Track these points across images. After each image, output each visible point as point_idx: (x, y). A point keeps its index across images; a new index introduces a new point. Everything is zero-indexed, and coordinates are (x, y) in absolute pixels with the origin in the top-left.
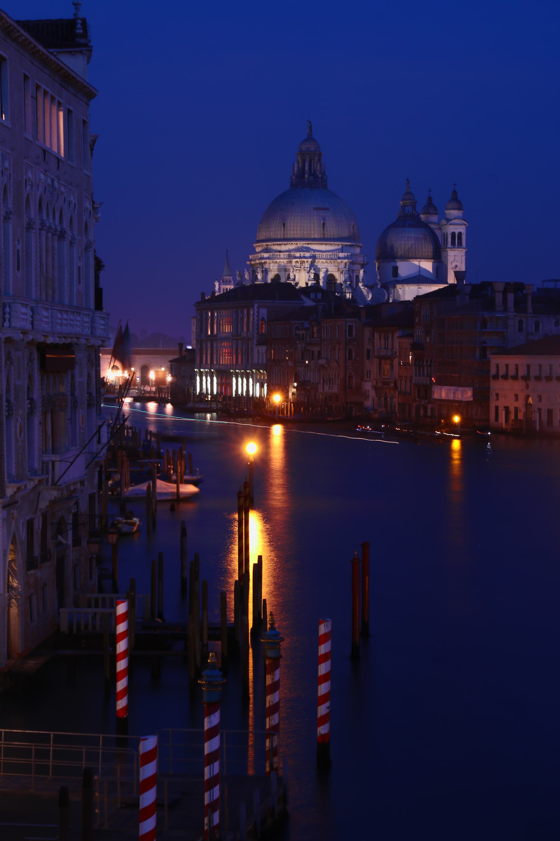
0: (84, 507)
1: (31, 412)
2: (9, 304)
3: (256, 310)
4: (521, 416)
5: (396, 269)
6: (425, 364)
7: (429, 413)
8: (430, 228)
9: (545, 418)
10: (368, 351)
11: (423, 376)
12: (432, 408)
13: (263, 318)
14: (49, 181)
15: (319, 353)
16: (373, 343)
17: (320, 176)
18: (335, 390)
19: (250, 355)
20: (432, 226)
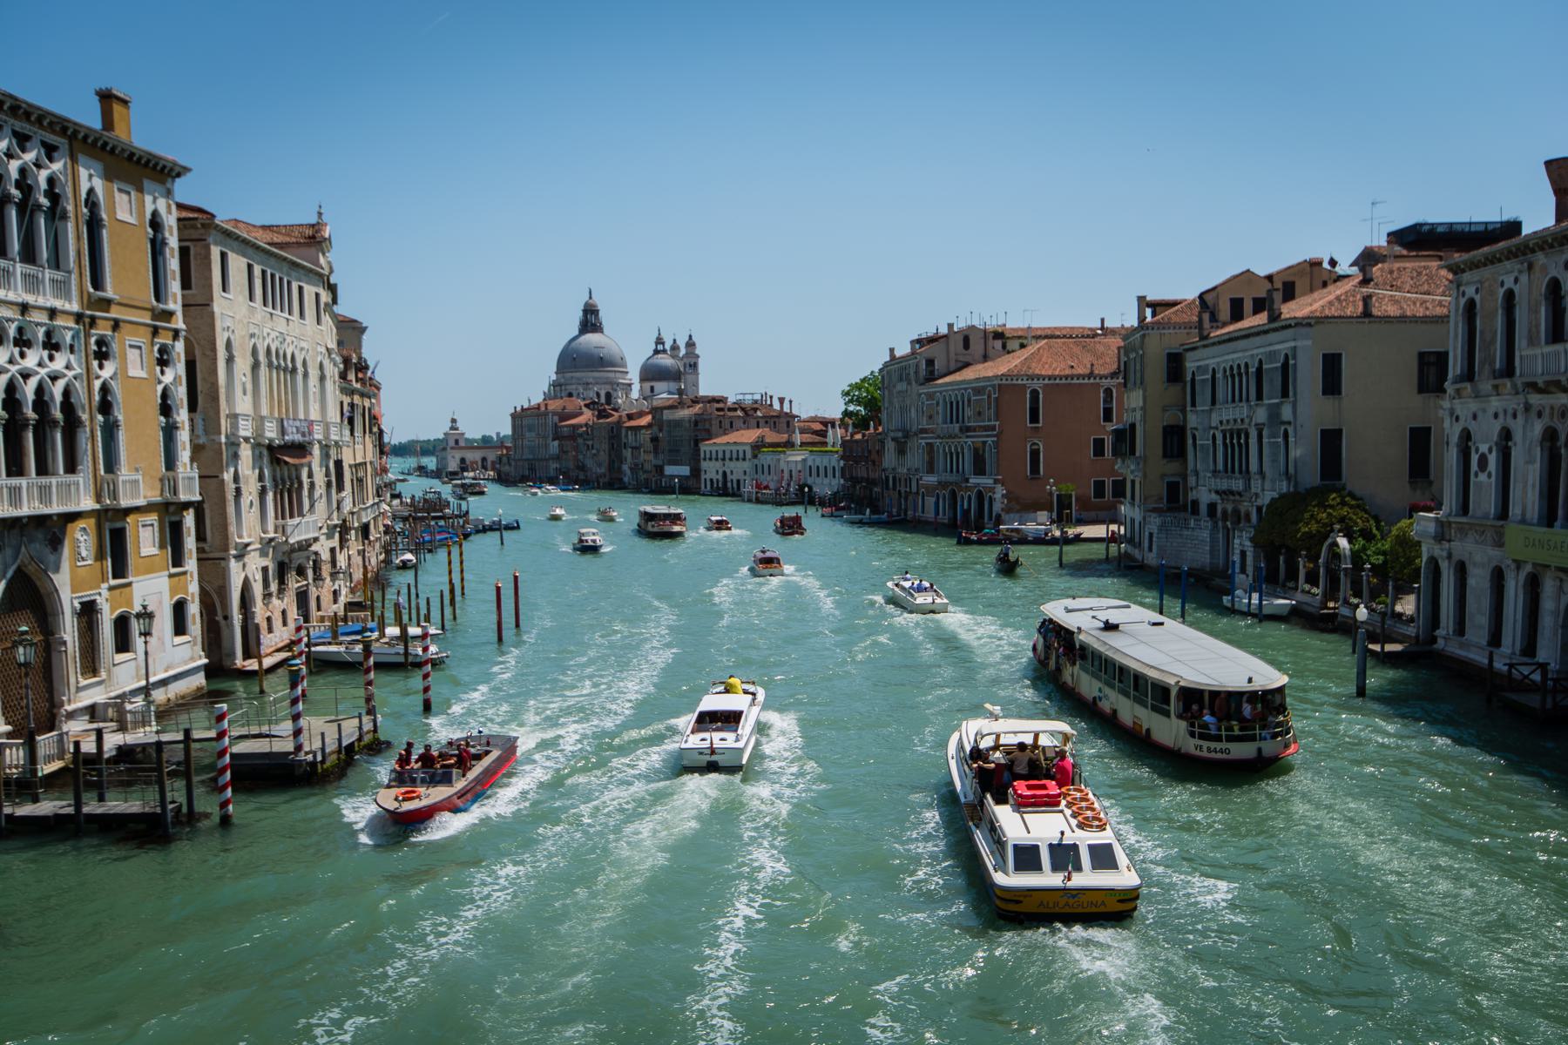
0: (325, 556)
1: (263, 493)
4: (720, 485)
5: (652, 389)
9: (735, 485)
18: (603, 470)
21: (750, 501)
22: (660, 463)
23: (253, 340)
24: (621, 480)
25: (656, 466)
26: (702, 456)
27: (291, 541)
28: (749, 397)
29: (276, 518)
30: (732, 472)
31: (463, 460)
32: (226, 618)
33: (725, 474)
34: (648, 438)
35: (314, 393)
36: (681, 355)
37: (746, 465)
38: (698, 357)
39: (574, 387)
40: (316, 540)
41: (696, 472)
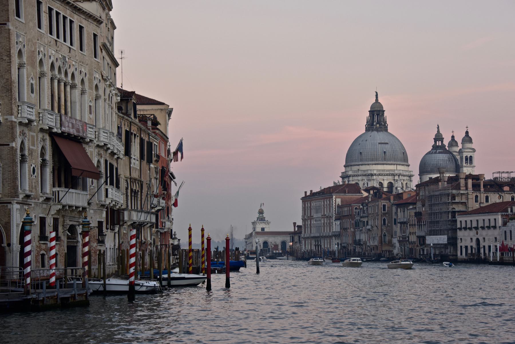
2: (21, 105)
3: (334, 199)
6: (422, 224)
7: (425, 253)
8: (452, 154)
9: (487, 252)
10: (395, 219)
11: (422, 231)
12: (426, 250)
13: (338, 204)
14: (60, 56)
15: (367, 222)
16: (397, 215)
17: (383, 124)
18: (376, 243)
19: (331, 227)
20: (454, 153)
21: (495, 263)
22: (422, 234)
23: (41, 55)
24: (390, 252)
25: (419, 237)
26: (459, 226)
27: (64, 202)
28: (505, 175)
29: (54, 186)
30: (484, 238)
31: (265, 243)
32: (9, 245)
33: (478, 240)
34: (413, 213)
35: (90, 106)
36: (458, 150)
37: (496, 233)
38: (474, 150)
39: (360, 178)
40: (84, 209)
41: (453, 241)
